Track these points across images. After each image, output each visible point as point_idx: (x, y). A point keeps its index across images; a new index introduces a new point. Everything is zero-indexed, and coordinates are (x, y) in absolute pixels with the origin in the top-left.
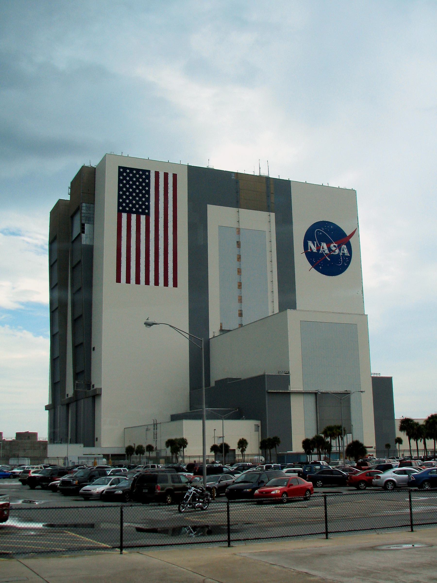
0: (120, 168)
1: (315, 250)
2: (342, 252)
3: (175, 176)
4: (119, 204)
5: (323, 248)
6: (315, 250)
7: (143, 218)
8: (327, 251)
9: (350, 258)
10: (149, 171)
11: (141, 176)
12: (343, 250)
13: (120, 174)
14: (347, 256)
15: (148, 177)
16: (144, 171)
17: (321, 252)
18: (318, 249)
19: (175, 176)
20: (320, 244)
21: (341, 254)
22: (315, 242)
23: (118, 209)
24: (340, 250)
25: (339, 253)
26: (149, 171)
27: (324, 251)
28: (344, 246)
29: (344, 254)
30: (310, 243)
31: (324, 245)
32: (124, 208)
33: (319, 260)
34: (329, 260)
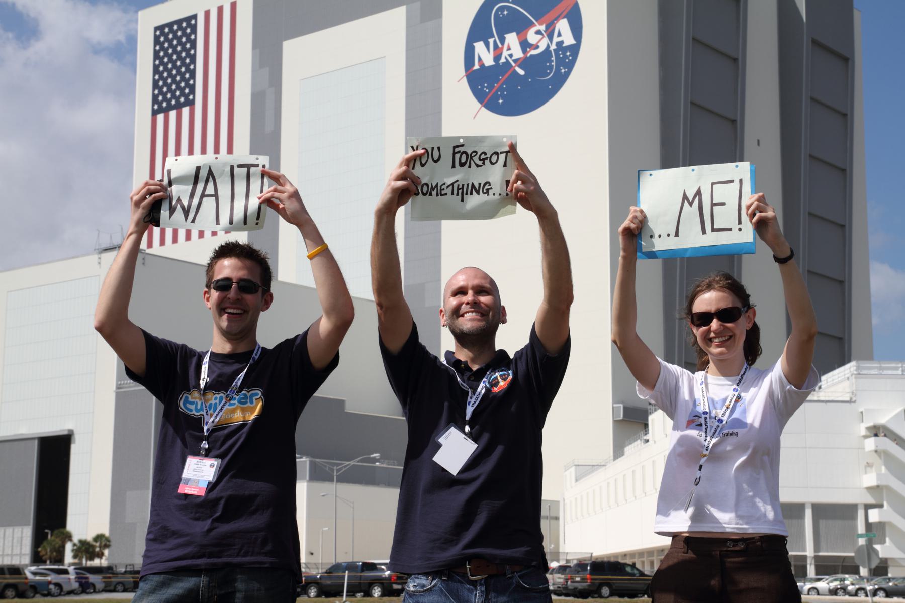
0: (156, 29)
1: (489, 61)
2: (556, 39)
3: (234, 6)
4: (155, 99)
5: (509, 49)
6: (489, 61)
7: (186, 111)
8: (518, 53)
9: (575, 49)
10: (195, 17)
11: (184, 30)
12: (559, 35)
13: (157, 41)
14: (570, 47)
15: (194, 29)
16: (188, 19)
17: (503, 60)
18: (497, 58)
19: (234, 6)
20: (503, 41)
21: (553, 47)
22: (491, 41)
23: (153, 109)
24: (550, 37)
25: (548, 47)
26: (195, 17)
27: (511, 56)
28: (563, 25)
29: (562, 42)
30: (479, 47)
31: (512, 39)
32: (160, 104)
33: (497, 81)
34: (521, 72)
